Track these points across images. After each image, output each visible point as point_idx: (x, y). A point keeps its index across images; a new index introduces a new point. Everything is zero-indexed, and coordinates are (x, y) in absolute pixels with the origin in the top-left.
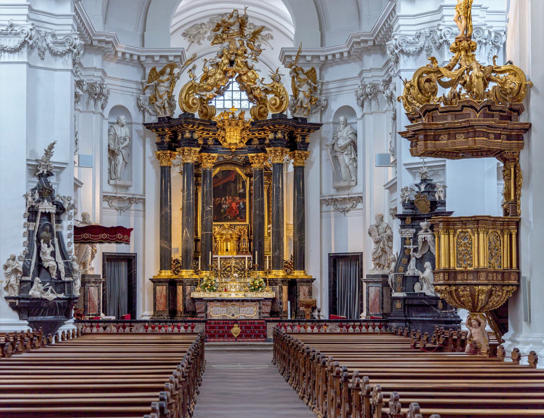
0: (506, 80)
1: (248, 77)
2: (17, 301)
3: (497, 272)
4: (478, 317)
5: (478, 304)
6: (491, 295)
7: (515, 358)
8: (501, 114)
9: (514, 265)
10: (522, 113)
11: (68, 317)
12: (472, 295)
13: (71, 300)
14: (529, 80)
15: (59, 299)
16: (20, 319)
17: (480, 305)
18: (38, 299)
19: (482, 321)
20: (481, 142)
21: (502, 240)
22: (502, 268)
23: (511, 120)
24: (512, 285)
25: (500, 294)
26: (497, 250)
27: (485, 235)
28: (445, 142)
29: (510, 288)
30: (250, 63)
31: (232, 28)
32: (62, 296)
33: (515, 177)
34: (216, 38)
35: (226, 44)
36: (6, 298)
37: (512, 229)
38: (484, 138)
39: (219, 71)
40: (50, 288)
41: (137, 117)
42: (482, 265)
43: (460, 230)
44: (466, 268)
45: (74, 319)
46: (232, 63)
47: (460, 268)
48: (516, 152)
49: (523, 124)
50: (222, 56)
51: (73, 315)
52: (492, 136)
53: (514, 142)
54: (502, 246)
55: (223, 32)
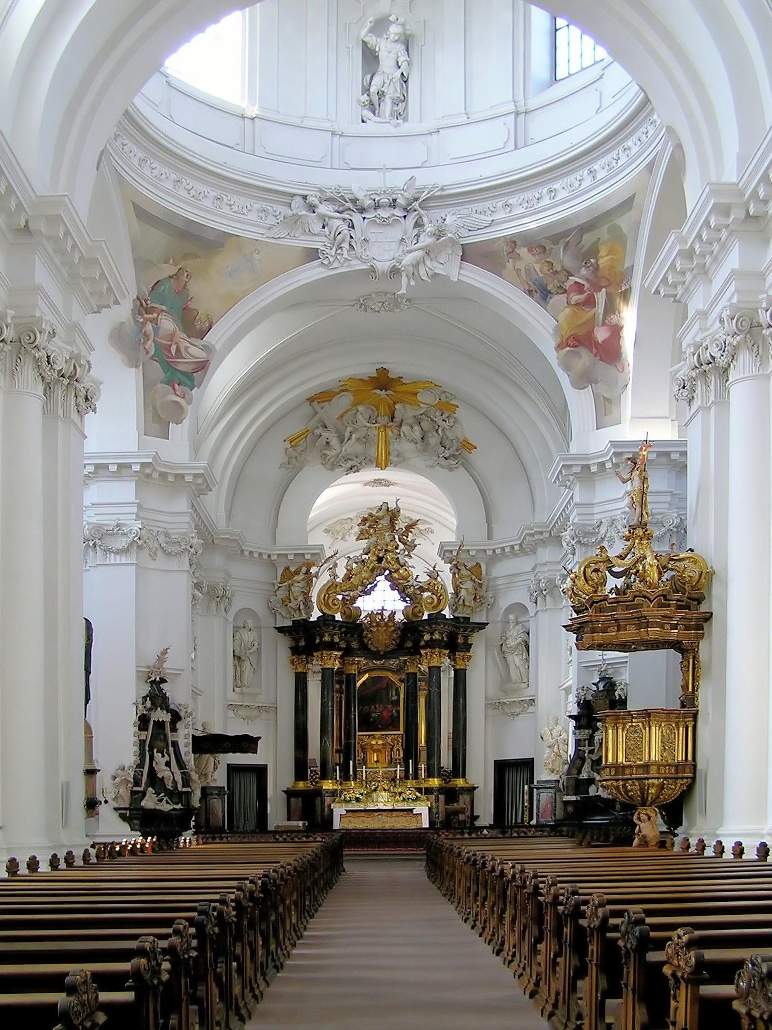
0: (685, 568)
1: (400, 574)
2: (128, 812)
3: (669, 765)
4: (649, 812)
5: (647, 798)
6: (663, 788)
7: (684, 847)
8: (679, 603)
9: (690, 758)
10: (703, 602)
11: (188, 828)
12: (642, 789)
13: (189, 811)
14: (711, 567)
15: (174, 809)
16: (131, 830)
17: (649, 799)
18: (151, 810)
19: (652, 815)
20: (654, 633)
21: (676, 733)
22: (676, 761)
23: (689, 609)
24: (687, 778)
25: (673, 787)
26: (671, 743)
27: (657, 728)
28: (614, 633)
29: (685, 780)
30: (402, 561)
31: (381, 522)
32: (179, 806)
33: (694, 668)
34: (362, 533)
35: (373, 539)
36: (115, 809)
37: (688, 721)
38: (658, 629)
39: (365, 568)
40: (166, 798)
41: (268, 622)
42: (653, 758)
43: (630, 724)
44: (635, 762)
45: (194, 830)
46: (380, 560)
47: (628, 763)
48: (695, 643)
49: (703, 613)
50: (369, 552)
51: (192, 827)
52: (668, 626)
53: (693, 632)
54: (676, 739)
55: (370, 527)
